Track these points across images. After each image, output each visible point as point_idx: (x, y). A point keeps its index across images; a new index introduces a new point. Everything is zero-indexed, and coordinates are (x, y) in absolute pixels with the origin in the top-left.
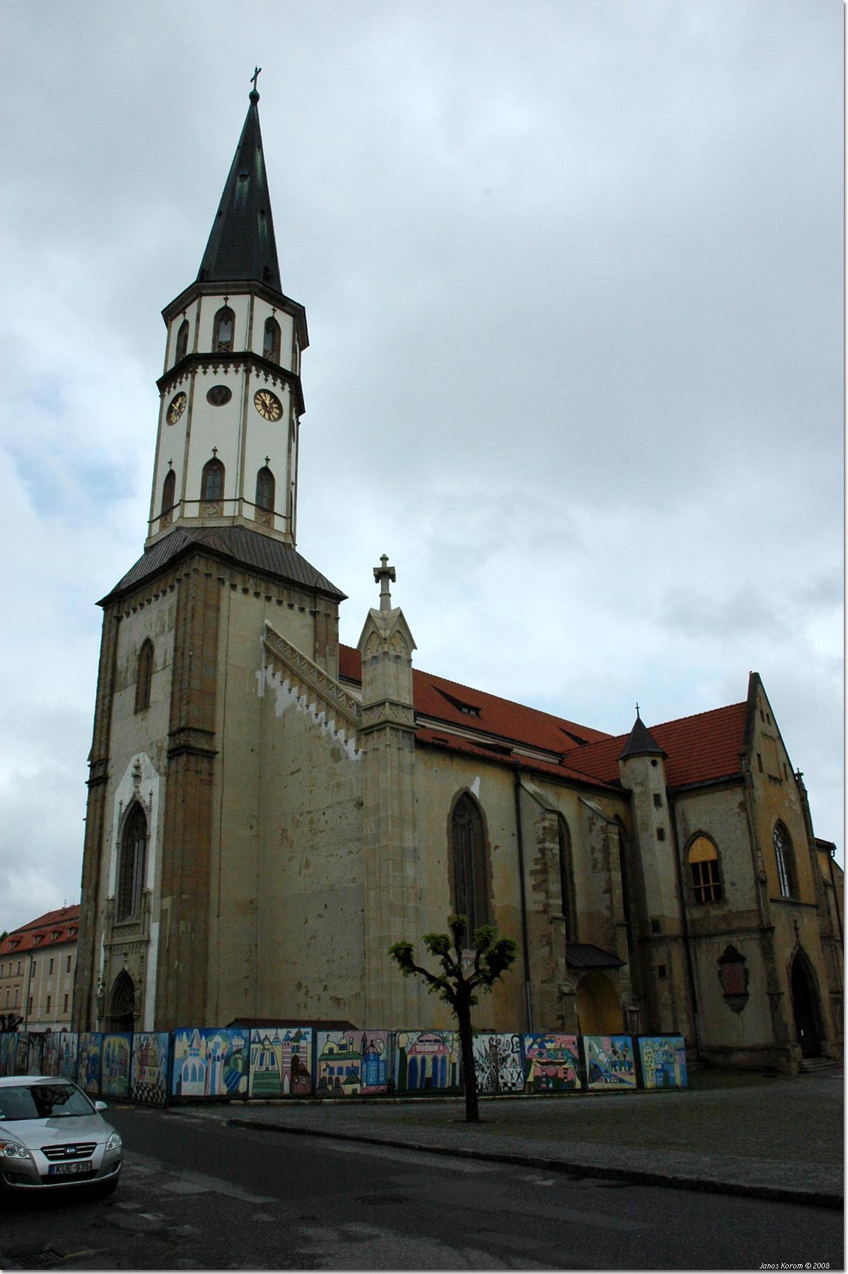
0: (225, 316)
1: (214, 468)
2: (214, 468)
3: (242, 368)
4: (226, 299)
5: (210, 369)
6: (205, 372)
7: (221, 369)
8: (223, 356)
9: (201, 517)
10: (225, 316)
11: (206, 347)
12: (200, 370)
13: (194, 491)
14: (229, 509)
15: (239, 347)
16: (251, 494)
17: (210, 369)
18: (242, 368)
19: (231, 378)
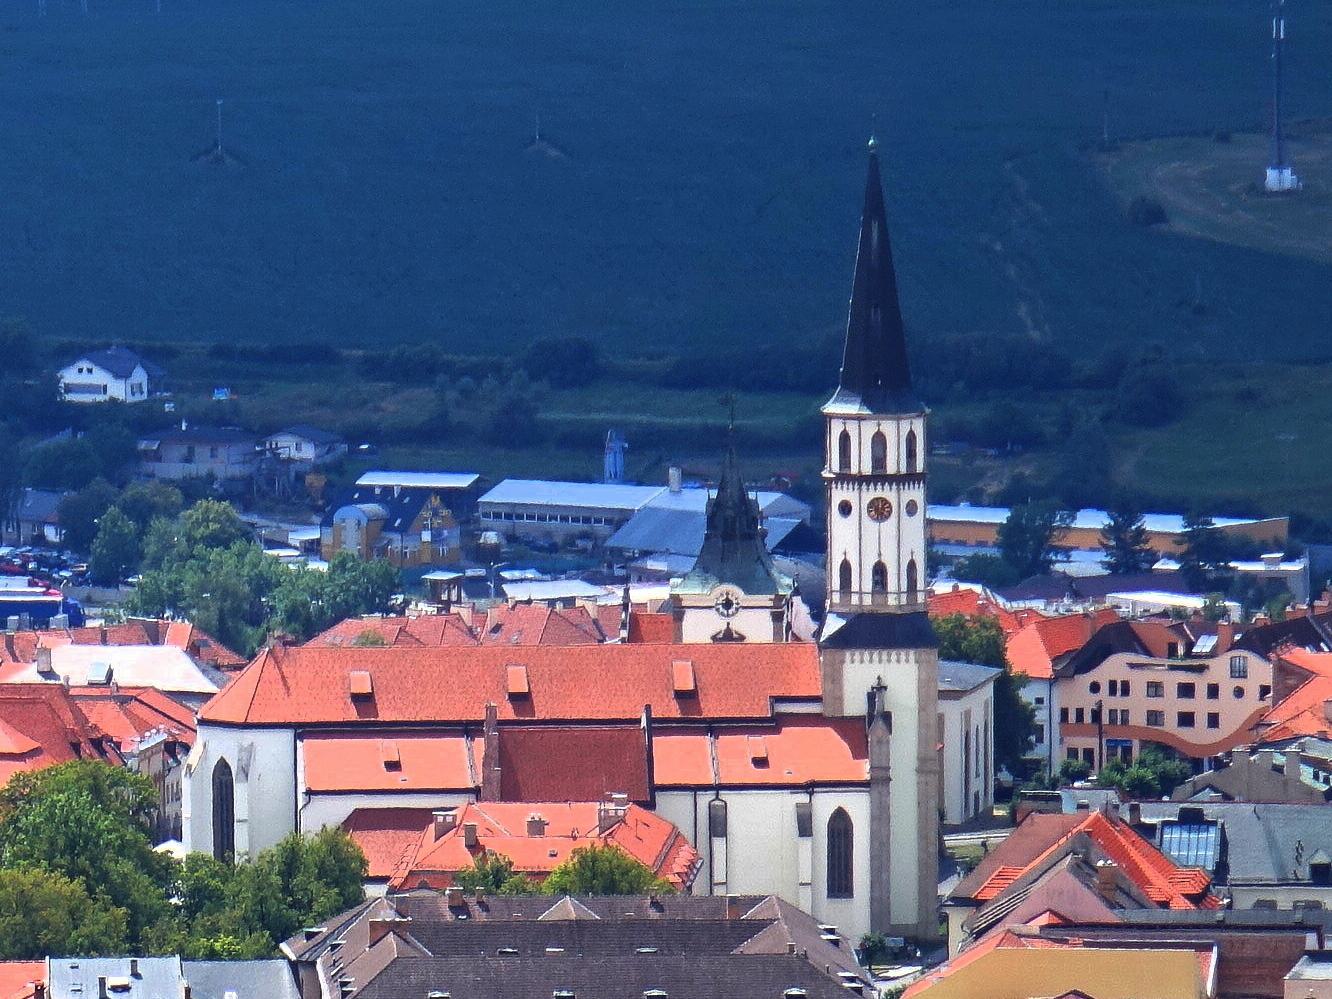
0: (879, 440)
1: (880, 571)
2: (880, 571)
3: (894, 486)
4: (879, 425)
5: (872, 486)
6: (868, 489)
7: (879, 487)
8: (879, 477)
9: (873, 604)
10: (879, 440)
11: (867, 469)
12: (864, 487)
13: (868, 586)
14: (892, 601)
15: (891, 469)
16: (904, 588)
17: (872, 486)
18: (894, 486)
19: (888, 493)
